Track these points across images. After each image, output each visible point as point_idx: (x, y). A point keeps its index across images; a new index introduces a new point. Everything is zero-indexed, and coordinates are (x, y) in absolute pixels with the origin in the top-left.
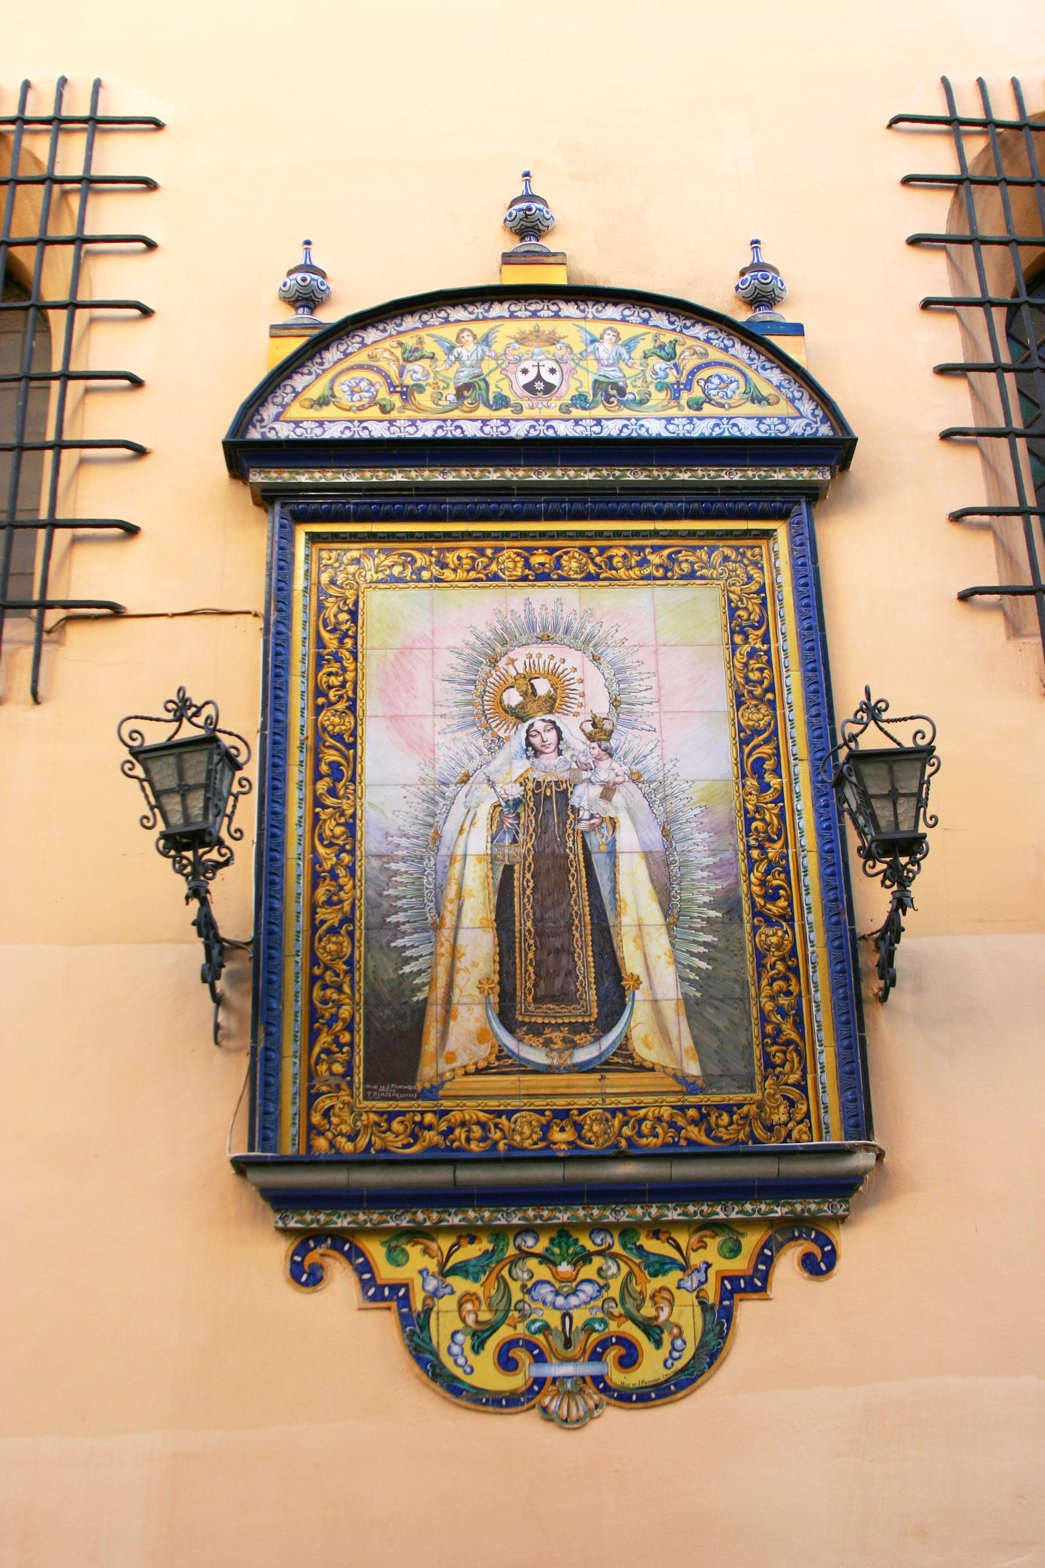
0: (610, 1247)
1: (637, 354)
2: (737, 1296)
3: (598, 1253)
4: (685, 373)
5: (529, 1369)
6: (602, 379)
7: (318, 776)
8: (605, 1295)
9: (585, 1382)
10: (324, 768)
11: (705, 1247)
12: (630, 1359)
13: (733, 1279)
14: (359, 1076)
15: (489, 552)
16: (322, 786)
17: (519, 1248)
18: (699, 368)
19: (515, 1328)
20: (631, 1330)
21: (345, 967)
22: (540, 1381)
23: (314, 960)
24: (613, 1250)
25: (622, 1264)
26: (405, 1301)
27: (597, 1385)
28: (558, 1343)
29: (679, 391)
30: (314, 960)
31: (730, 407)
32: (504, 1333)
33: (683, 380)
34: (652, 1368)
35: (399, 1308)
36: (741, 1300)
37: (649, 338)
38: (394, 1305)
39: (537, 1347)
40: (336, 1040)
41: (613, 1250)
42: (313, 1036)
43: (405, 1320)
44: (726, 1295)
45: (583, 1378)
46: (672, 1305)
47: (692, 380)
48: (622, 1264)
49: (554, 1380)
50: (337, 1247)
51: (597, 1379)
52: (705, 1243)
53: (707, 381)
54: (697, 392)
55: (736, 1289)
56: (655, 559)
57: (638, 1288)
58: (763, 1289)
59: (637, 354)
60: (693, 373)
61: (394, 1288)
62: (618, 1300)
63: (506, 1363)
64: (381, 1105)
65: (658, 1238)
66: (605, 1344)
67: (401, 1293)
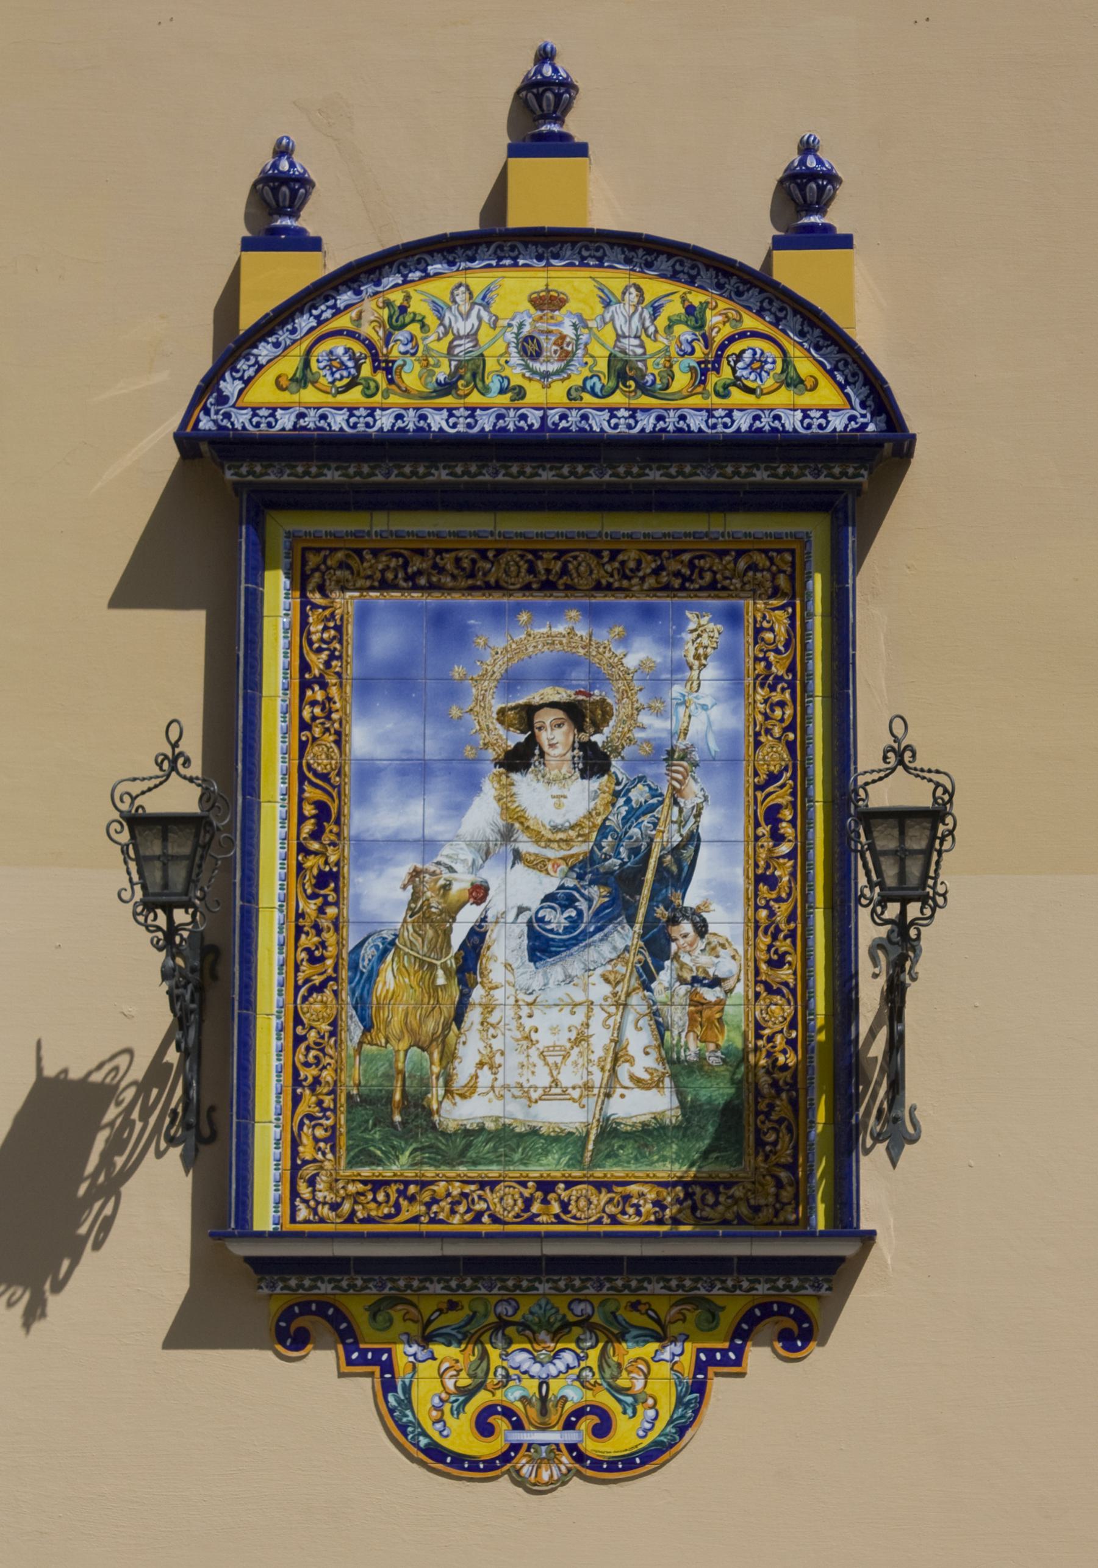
0: (589, 1317)
1: (662, 322)
2: (711, 1370)
3: (575, 1324)
4: (715, 346)
5: (504, 1434)
6: (620, 355)
7: (302, 819)
8: (583, 1364)
9: (559, 1450)
10: (309, 810)
11: (684, 1320)
12: (603, 1429)
13: (710, 1353)
14: (343, 1141)
15: (491, 554)
16: (308, 827)
17: (499, 1317)
18: (731, 339)
19: (494, 1395)
20: (605, 1399)
21: (329, 1028)
22: (516, 1447)
23: (298, 1021)
24: (592, 1320)
25: (598, 1332)
26: (388, 1367)
27: (570, 1453)
28: (533, 1413)
29: (704, 373)
30: (298, 1021)
31: (762, 394)
32: (482, 1398)
33: (711, 358)
34: (627, 1436)
35: (382, 1373)
36: (717, 1374)
37: (677, 298)
38: (377, 1369)
39: (515, 1414)
40: (320, 1103)
41: (592, 1320)
42: (296, 1100)
43: (388, 1386)
44: (700, 1367)
45: (557, 1445)
46: (646, 1376)
47: (721, 356)
48: (598, 1332)
49: (530, 1446)
50: (321, 1311)
51: (572, 1447)
52: (684, 1315)
53: (739, 357)
54: (726, 372)
55: (712, 1361)
56: (673, 566)
57: (615, 1359)
58: (738, 1362)
59: (662, 322)
60: (723, 347)
61: (378, 1352)
62: (596, 1370)
63: (484, 1428)
64: (366, 1172)
65: (638, 1310)
66: (580, 1413)
67: (385, 1357)
